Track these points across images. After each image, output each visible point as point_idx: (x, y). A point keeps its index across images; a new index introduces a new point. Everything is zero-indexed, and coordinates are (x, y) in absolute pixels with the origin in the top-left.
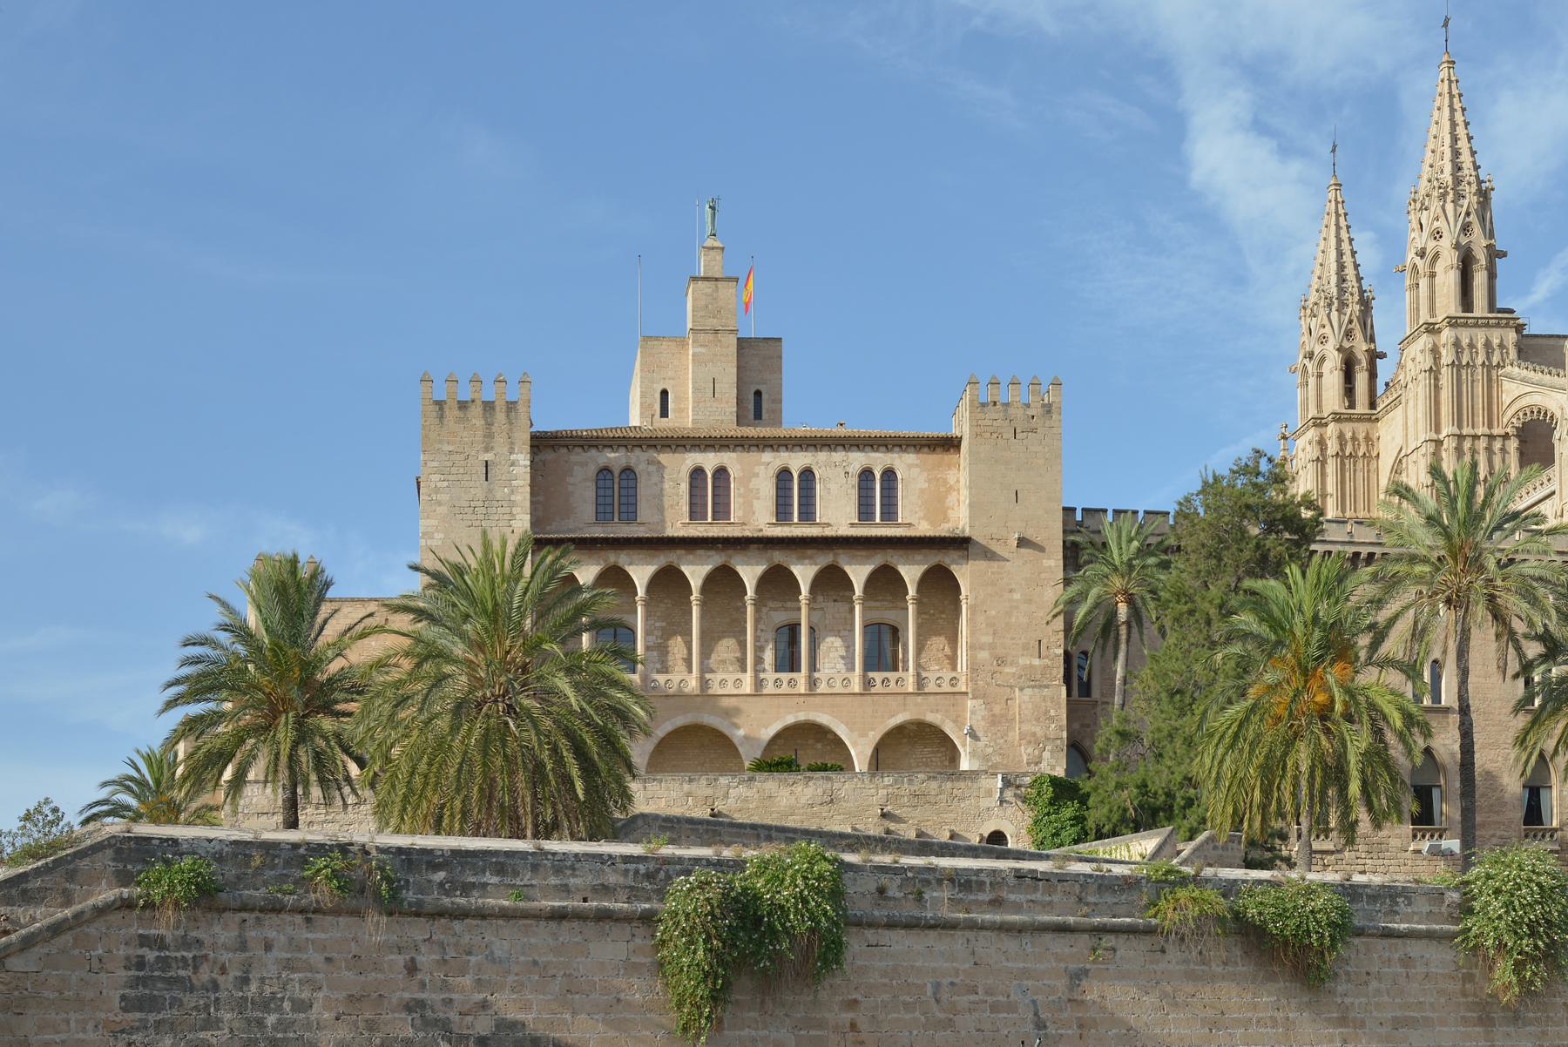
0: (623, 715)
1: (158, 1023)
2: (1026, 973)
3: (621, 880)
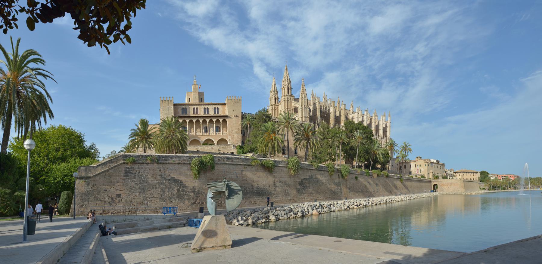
0: (186, 138)
1: (128, 178)
2: (236, 170)
3: (186, 159)
